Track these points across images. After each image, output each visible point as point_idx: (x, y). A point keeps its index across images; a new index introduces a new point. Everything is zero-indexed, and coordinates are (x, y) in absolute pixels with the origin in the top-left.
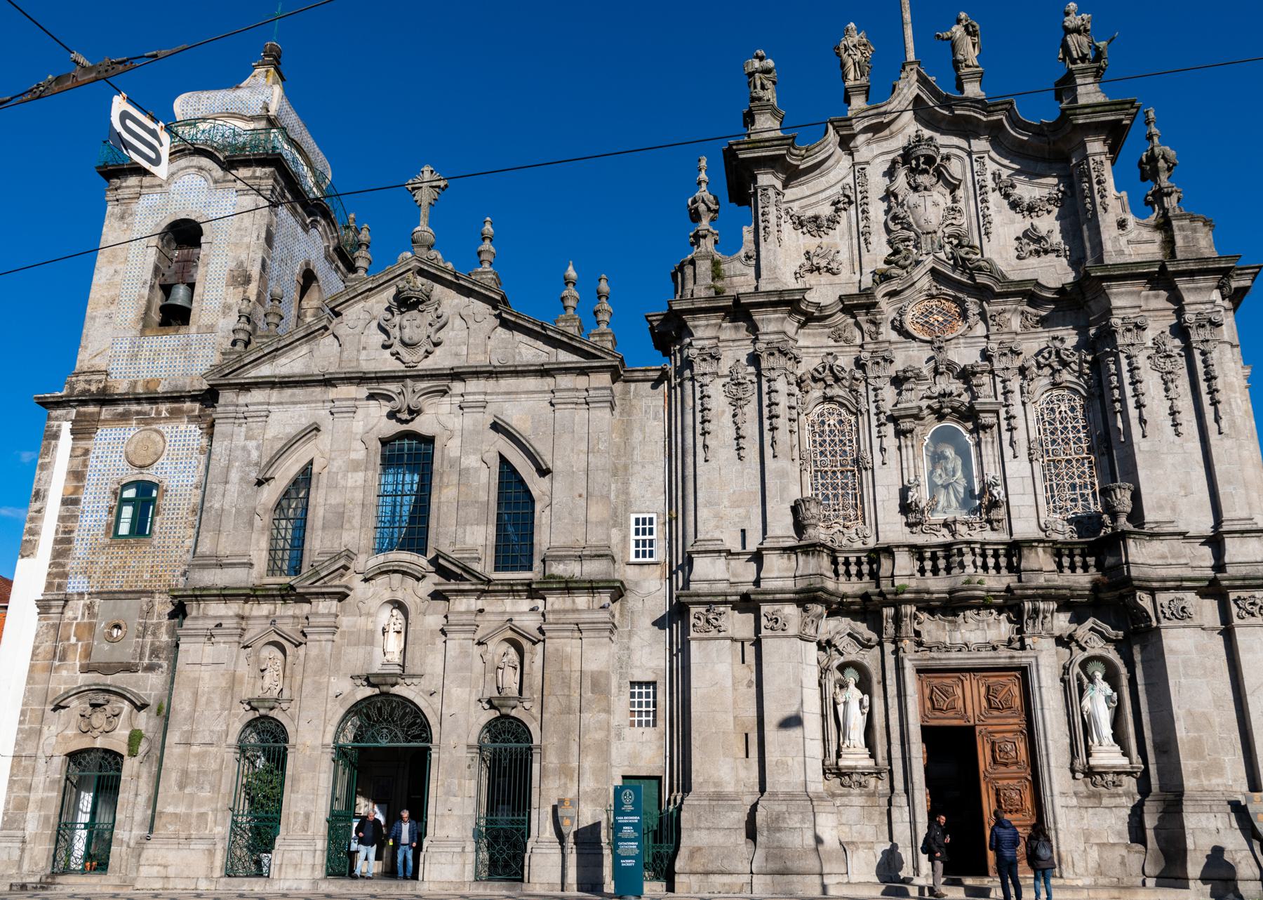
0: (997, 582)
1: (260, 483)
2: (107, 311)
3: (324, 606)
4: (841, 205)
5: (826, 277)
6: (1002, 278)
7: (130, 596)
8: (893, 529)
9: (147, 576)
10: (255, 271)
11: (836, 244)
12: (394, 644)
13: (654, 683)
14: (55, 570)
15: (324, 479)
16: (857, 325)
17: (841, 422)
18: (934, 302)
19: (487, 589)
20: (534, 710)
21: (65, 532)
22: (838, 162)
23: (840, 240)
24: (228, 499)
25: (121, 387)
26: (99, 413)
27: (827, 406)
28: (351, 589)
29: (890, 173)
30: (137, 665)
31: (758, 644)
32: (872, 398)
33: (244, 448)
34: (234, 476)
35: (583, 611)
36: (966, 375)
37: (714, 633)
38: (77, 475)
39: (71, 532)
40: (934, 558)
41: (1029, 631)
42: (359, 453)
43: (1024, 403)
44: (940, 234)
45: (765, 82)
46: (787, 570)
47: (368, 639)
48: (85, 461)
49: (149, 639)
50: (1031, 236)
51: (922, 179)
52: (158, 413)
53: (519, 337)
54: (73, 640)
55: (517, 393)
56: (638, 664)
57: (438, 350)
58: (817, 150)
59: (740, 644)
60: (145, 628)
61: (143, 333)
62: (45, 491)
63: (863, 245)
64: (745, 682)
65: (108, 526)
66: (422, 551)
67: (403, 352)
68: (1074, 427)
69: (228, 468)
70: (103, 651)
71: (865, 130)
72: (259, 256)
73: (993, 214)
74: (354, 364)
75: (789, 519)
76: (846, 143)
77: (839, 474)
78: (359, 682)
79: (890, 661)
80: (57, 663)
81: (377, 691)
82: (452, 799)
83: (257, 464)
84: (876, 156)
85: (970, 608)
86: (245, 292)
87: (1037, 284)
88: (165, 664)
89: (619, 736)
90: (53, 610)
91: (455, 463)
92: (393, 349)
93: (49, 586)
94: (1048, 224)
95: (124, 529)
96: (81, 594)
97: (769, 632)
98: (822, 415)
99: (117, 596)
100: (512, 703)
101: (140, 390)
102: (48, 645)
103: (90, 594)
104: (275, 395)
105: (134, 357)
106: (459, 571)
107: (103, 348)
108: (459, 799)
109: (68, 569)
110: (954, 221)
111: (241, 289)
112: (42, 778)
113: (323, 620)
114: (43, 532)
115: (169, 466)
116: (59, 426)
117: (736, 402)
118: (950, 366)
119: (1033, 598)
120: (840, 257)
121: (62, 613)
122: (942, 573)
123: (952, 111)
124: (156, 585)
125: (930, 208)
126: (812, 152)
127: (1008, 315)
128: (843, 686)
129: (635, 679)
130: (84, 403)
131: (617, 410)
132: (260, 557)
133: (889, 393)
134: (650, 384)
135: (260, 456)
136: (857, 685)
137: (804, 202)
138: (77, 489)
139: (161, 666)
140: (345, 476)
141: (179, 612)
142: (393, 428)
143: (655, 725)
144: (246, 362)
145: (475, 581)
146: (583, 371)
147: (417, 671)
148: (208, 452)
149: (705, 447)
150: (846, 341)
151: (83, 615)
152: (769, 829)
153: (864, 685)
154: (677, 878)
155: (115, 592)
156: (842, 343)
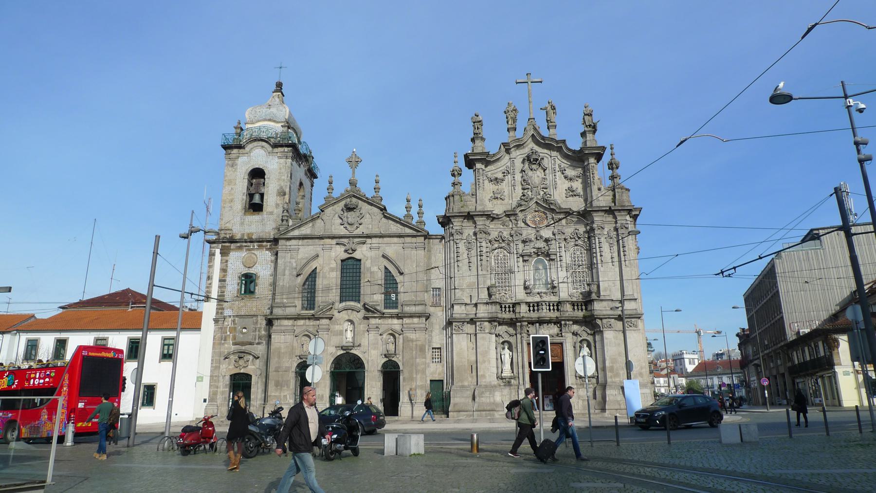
0: (554, 315)
1: (298, 275)
2: (230, 205)
3: (325, 322)
4: (505, 174)
5: (499, 201)
6: (560, 208)
7: (249, 317)
8: (521, 295)
9: (254, 309)
10: (287, 190)
11: (503, 189)
12: (349, 335)
13: (440, 348)
14: (219, 307)
15: (321, 274)
16: (510, 220)
17: (504, 256)
19: (383, 316)
20: (400, 358)
21: (221, 292)
22: (504, 157)
23: (505, 187)
24: (285, 281)
26: (230, 246)
27: (499, 250)
28: (333, 315)
29: (523, 162)
30: (254, 342)
31: (476, 335)
32: (515, 248)
33: (290, 262)
34: (287, 272)
35: (416, 324)
36: (547, 241)
37: (461, 332)
38: (224, 270)
39: (224, 292)
40: (534, 306)
41: (563, 331)
42: (333, 265)
43: (565, 251)
44: (539, 188)
45: (479, 126)
46: (486, 310)
47: (341, 333)
48: (227, 265)
49: (257, 333)
50: (570, 189)
51: (534, 167)
52: (254, 246)
53: (391, 222)
54: (228, 333)
55: (390, 244)
56: (435, 341)
57: (361, 226)
59: (469, 335)
60: (256, 329)
61: (245, 214)
62: (212, 276)
63: (513, 190)
64: (471, 348)
65: (238, 290)
66: (359, 301)
67: (348, 226)
68: (581, 260)
69: (284, 270)
70: (240, 338)
72: (288, 184)
73: (557, 180)
74: (329, 231)
75: (486, 292)
77: (503, 274)
78: (338, 348)
79: (519, 341)
80: (223, 342)
81: (345, 352)
82: (373, 389)
83: (296, 268)
84: (518, 155)
85: (545, 323)
86: (284, 199)
87: (570, 209)
88: (264, 342)
89: (429, 366)
90: (220, 322)
91: (369, 269)
92: (345, 226)
93: (217, 313)
94: (578, 185)
95: (243, 292)
96: (230, 316)
97: (479, 332)
98: (498, 253)
99: (244, 317)
100: (393, 356)
101: (246, 237)
103: (233, 316)
104: (301, 242)
105: (242, 224)
106: (373, 310)
107: (230, 219)
108: (375, 389)
109: (224, 306)
110: (544, 183)
111: (282, 198)
112: (222, 384)
113: (324, 326)
114: (213, 292)
115: (259, 268)
116: (215, 251)
117: (469, 249)
118: (541, 237)
119: (565, 320)
120: (505, 194)
121: (223, 323)
122: (536, 311)
123: (545, 141)
124: (259, 313)
125: (538, 178)
128: (504, 349)
129: (434, 347)
131: (426, 249)
132: (299, 303)
133: (521, 246)
134: (438, 240)
135: (297, 265)
136: (508, 349)
138: (224, 276)
139: (262, 343)
140: (329, 274)
141: (270, 323)
142: (346, 256)
143: (441, 362)
144: (290, 229)
145: (379, 313)
148: (276, 262)
149: (458, 266)
150: (506, 226)
151: (231, 324)
152: (479, 397)
153: (510, 349)
154: (449, 413)
155: (243, 315)
156: (505, 227)
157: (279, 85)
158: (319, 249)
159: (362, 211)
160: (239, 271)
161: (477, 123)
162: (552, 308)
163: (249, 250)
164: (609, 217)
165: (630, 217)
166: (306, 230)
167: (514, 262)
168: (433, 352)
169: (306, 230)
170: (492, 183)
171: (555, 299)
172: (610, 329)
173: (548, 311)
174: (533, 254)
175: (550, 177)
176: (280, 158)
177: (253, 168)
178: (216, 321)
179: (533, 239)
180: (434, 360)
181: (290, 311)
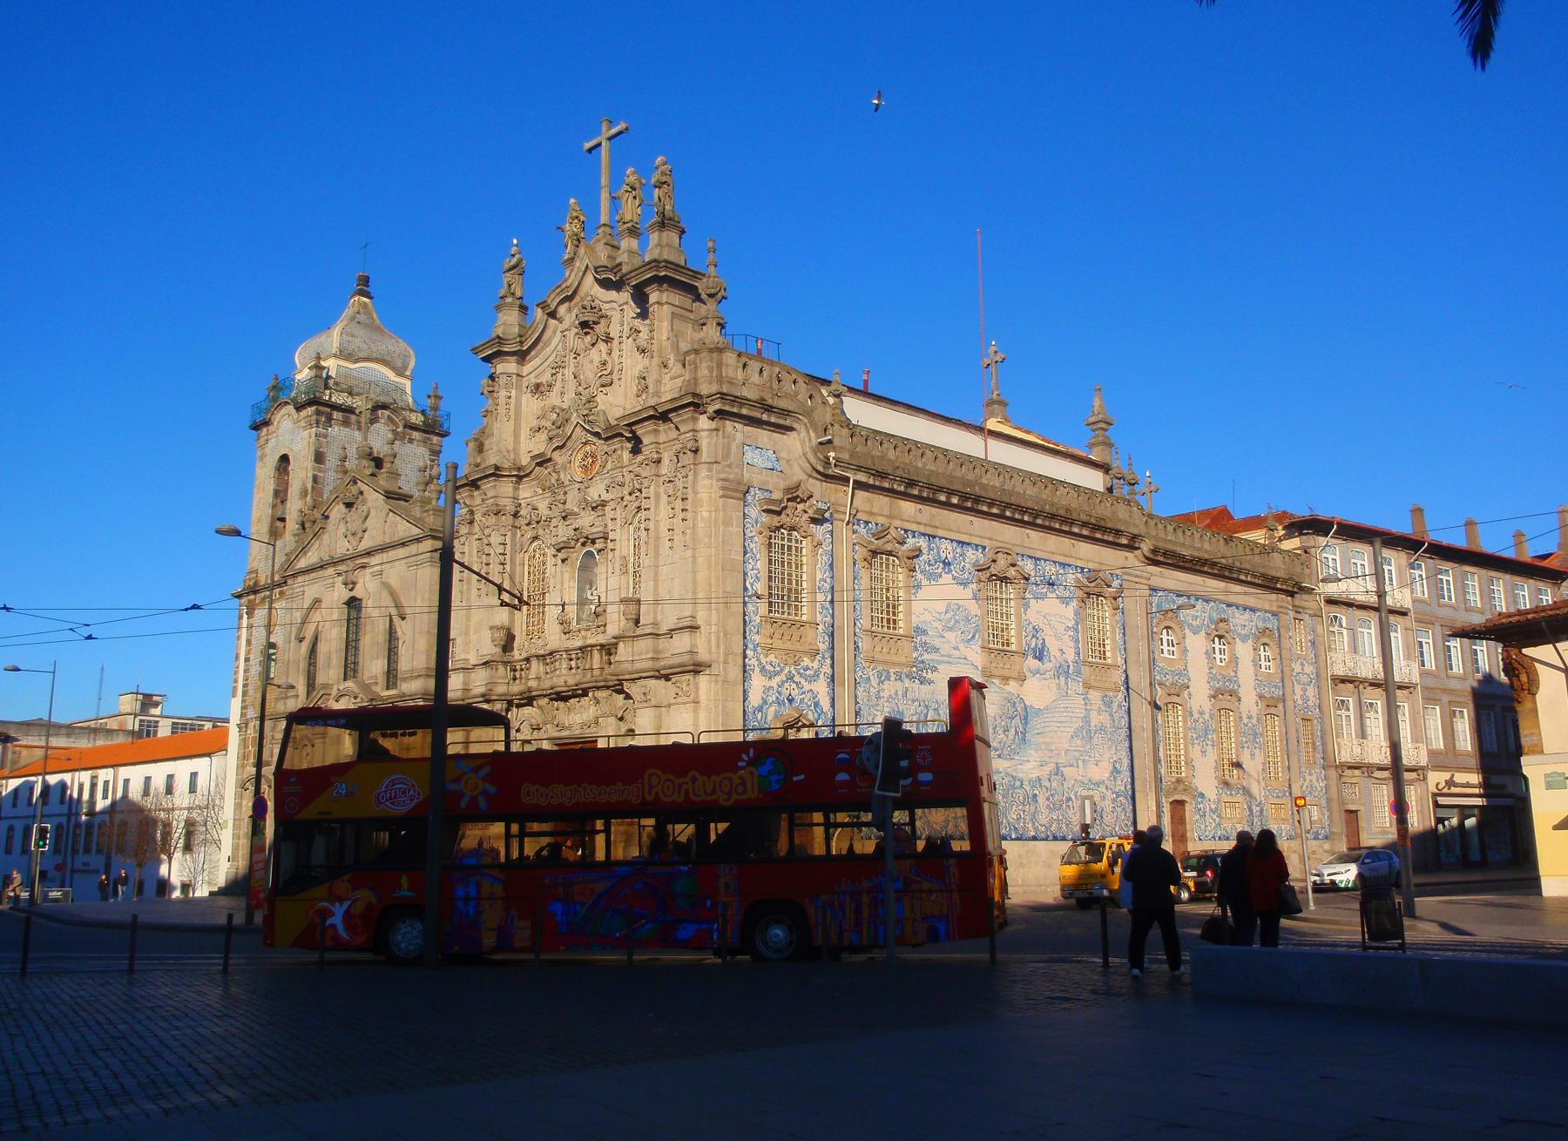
1: (301, 641)
10: (309, 486)
18: (588, 448)
38: (249, 642)
57: (366, 534)
58: (529, 332)
71: (562, 302)
76: (553, 315)
93: (242, 713)
98: (534, 551)
110: (604, 372)
126: (527, 336)
127: (619, 452)
138: (250, 650)
146: (418, 540)
159: (369, 504)
164: (670, 429)
167: (552, 567)
170: (536, 396)
171: (601, 639)
172: (646, 705)
173: (564, 672)
174: (573, 543)
175: (616, 353)
177: (278, 457)
179: (576, 510)
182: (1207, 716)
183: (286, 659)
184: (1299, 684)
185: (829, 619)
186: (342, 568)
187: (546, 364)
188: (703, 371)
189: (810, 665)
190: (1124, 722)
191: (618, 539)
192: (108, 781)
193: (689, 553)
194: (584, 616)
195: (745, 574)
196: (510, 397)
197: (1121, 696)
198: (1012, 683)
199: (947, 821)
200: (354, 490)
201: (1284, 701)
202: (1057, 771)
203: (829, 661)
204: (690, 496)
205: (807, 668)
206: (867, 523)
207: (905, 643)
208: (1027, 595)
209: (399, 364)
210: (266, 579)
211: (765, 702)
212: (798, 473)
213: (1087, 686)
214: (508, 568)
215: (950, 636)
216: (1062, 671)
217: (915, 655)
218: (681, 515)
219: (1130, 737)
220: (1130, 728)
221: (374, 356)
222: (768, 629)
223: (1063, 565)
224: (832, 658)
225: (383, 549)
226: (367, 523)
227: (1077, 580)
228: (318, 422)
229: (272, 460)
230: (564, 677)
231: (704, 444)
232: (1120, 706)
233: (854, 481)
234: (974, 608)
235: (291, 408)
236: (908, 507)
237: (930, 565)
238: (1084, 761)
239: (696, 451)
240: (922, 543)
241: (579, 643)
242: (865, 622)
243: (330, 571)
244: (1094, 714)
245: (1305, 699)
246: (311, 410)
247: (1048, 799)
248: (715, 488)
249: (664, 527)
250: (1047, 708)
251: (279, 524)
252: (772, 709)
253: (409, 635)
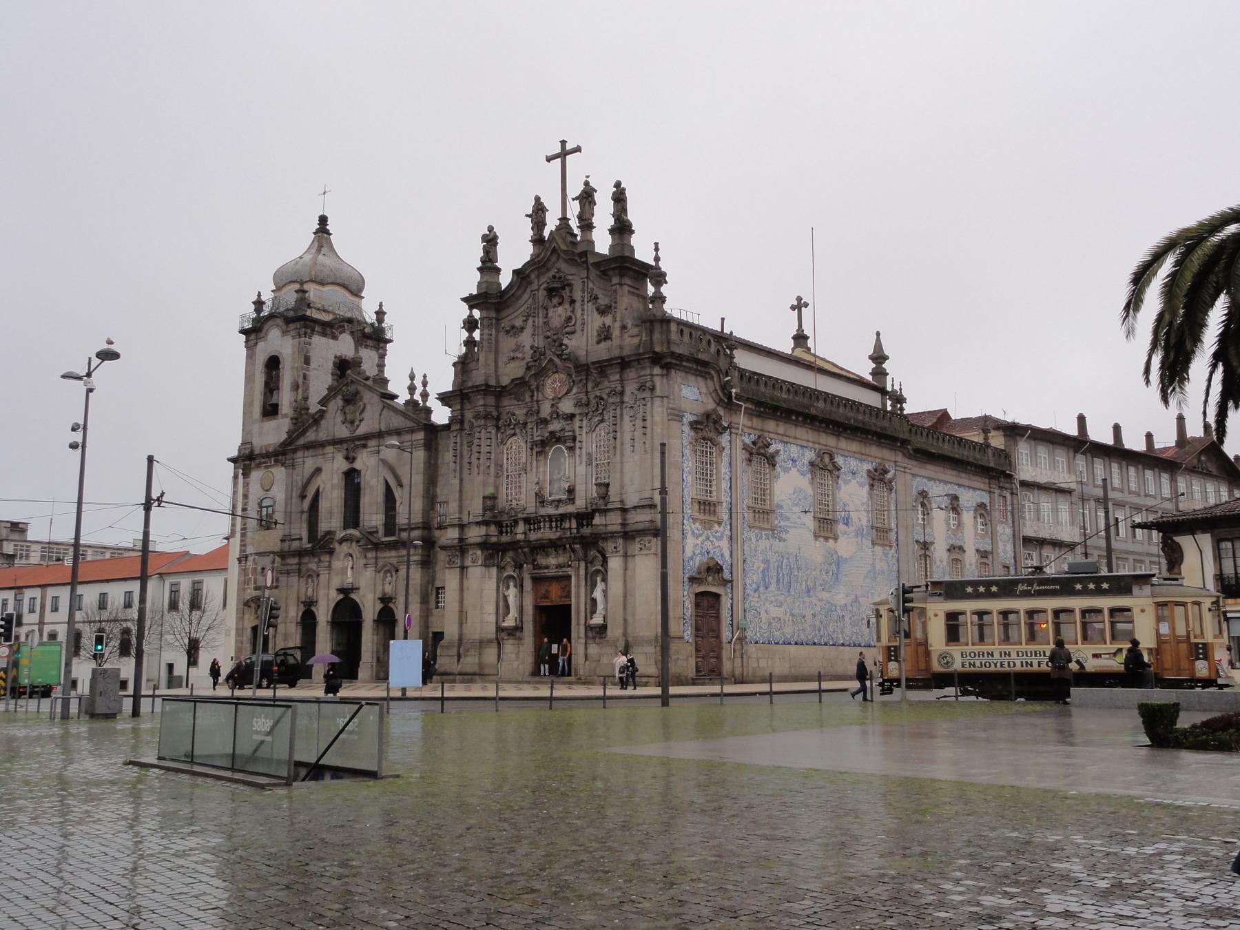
10: (300, 382)
18: (556, 375)
19: (377, 546)
25: (257, 451)
33: (297, 481)
34: (294, 495)
38: (245, 496)
42: (335, 481)
57: (362, 424)
73: (585, 317)
93: (241, 551)
96: (251, 554)
101: (264, 452)
102: (242, 578)
105: (260, 433)
115: (276, 490)
130: (244, 460)
132: (305, 535)
137: (510, 318)
138: (245, 505)
146: (412, 431)
147: (357, 586)
153: (515, 586)
156: (520, 403)
157: (323, 220)
158: (319, 461)
160: (259, 496)
161: (490, 241)
162: (554, 524)
163: (267, 467)
164: (631, 371)
165: (662, 367)
166: (311, 436)
168: (438, 593)
169: (311, 436)
170: (511, 333)
171: (570, 509)
173: (547, 530)
176: (294, 337)
178: (239, 560)
179: (548, 418)
180: (440, 605)
181: (295, 545)
182: (945, 563)
183: (289, 510)
184: (1001, 540)
185: (729, 499)
186: (345, 446)
187: (520, 311)
188: (656, 336)
189: (718, 529)
190: (895, 568)
191: (584, 440)
192: (34, 599)
193: (648, 456)
194: (554, 491)
195: (683, 470)
196: (491, 335)
197: (894, 549)
198: (830, 541)
199: (794, 632)
200: (352, 388)
201: (992, 553)
202: (856, 600)
203: (729, 527)
204: (649, 418)
205: (717, 532)
206: (749, 434)
207: (772, 516)
208: (840, 481)
209: (354, 288)
210: (261, 447)
211: (694, 554)
212: (711, 405)
213: (873, 544)
214: (493, 456)
215: (795, 509)
216: (859, 532)
217: (776, 523)
218: (642, 430)
219: (898, 577)
220: (898, 571)
221: (338, 281)
222: (696, 506)
223: (861, 460)
224: (731, 524)
225: (380, 435)
226: (363, 415)
227: (869, 471)
228: (305, 334)
229: (261, 358)
230: (546, 533)
231: (658, 381)
232: (893, 557)
233: (745, 408)
234: (809, 490)
235: (279, 321)
236: (771, 425)
237: (785, 462)
238: (872, 593)
239: (653, 389)
240: (780, 446)
241: (551, 510)
242: (748, 501)
243: (329, 449)
244: (878, 561)
245: (1005, 551)
246: (298, 325)
247: (851, 618)
248: (665, 413)
249: (627, 437)
250: (851, 557)
251: (268, 407)
252: (698, 558)
253: (406, 496)
